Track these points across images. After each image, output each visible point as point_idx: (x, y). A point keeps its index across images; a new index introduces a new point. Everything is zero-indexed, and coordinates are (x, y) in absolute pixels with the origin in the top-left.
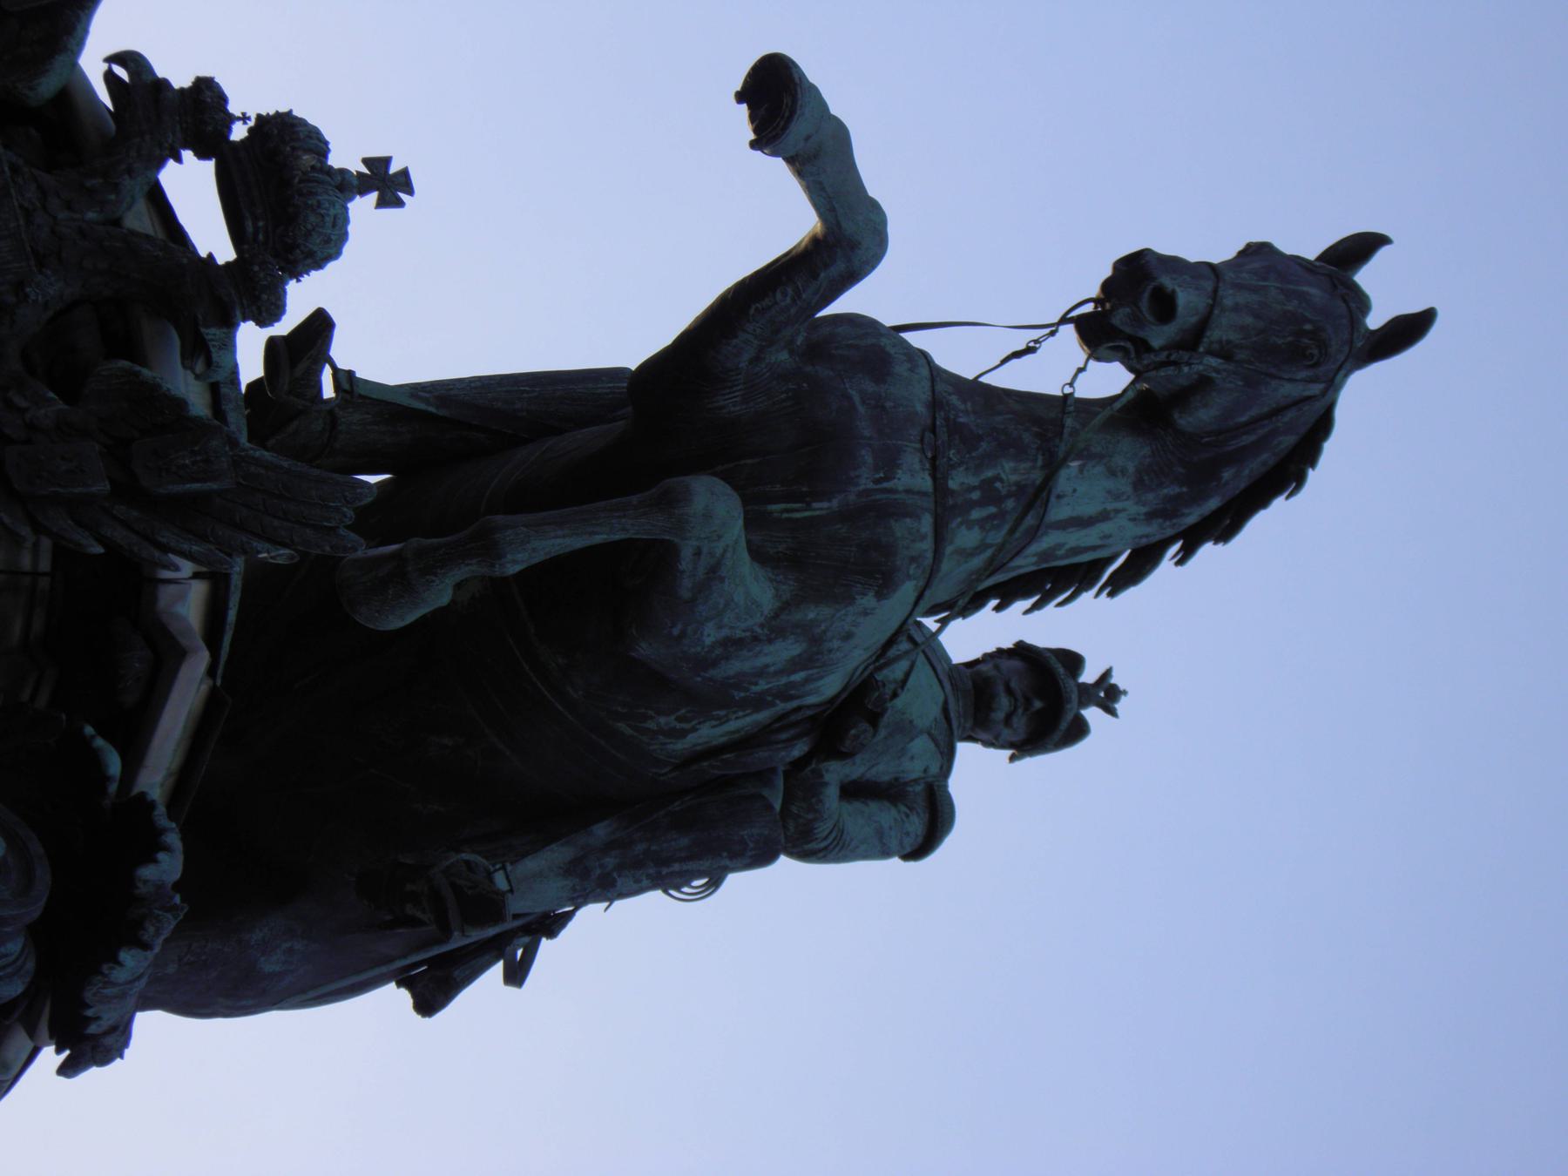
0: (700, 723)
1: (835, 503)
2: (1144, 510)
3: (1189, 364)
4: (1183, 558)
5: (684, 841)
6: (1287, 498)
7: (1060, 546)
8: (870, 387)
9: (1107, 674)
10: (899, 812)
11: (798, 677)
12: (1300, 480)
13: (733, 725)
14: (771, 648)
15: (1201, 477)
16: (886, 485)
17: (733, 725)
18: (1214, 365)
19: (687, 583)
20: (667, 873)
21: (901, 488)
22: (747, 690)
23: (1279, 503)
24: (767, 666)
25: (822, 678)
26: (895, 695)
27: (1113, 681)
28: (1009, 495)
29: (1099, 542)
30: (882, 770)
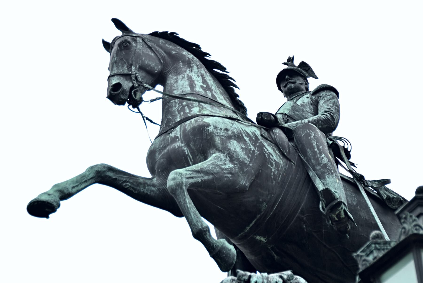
0: (272, 160)
1: (185, 149)
2: (188, 70)
3: (135, 74)
4: (206, 54)
5: (308, 150)
6: (178, 35)
7: (202, 87)
8: (158, 153)
9: (284, 64)
10: (320, 100)
11: (247, 139)
12: (173, 34)
13: (271, 150)
14: (232, 149)
15: (175, 59)
16: (179, 138)
17: (271, 150)
18: (134, 68)
19: (206, 178)
20: (318, 151)
21: (180, 133)
22: (254, 151)
23: (181, 36)
24: (242, 148)
25: (247, 133)
26: (286, 114)
27: (286, 61)
28: (182, 105)
29: (200, 77)
30: (309, 109)
